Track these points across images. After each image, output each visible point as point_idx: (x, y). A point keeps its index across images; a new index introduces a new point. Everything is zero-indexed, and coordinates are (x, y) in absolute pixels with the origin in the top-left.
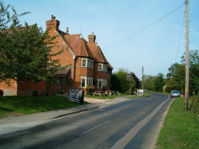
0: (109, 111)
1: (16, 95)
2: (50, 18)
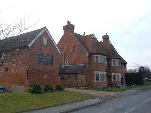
0: (86, 100)
1: (74, 32)
2: (66, 24)
